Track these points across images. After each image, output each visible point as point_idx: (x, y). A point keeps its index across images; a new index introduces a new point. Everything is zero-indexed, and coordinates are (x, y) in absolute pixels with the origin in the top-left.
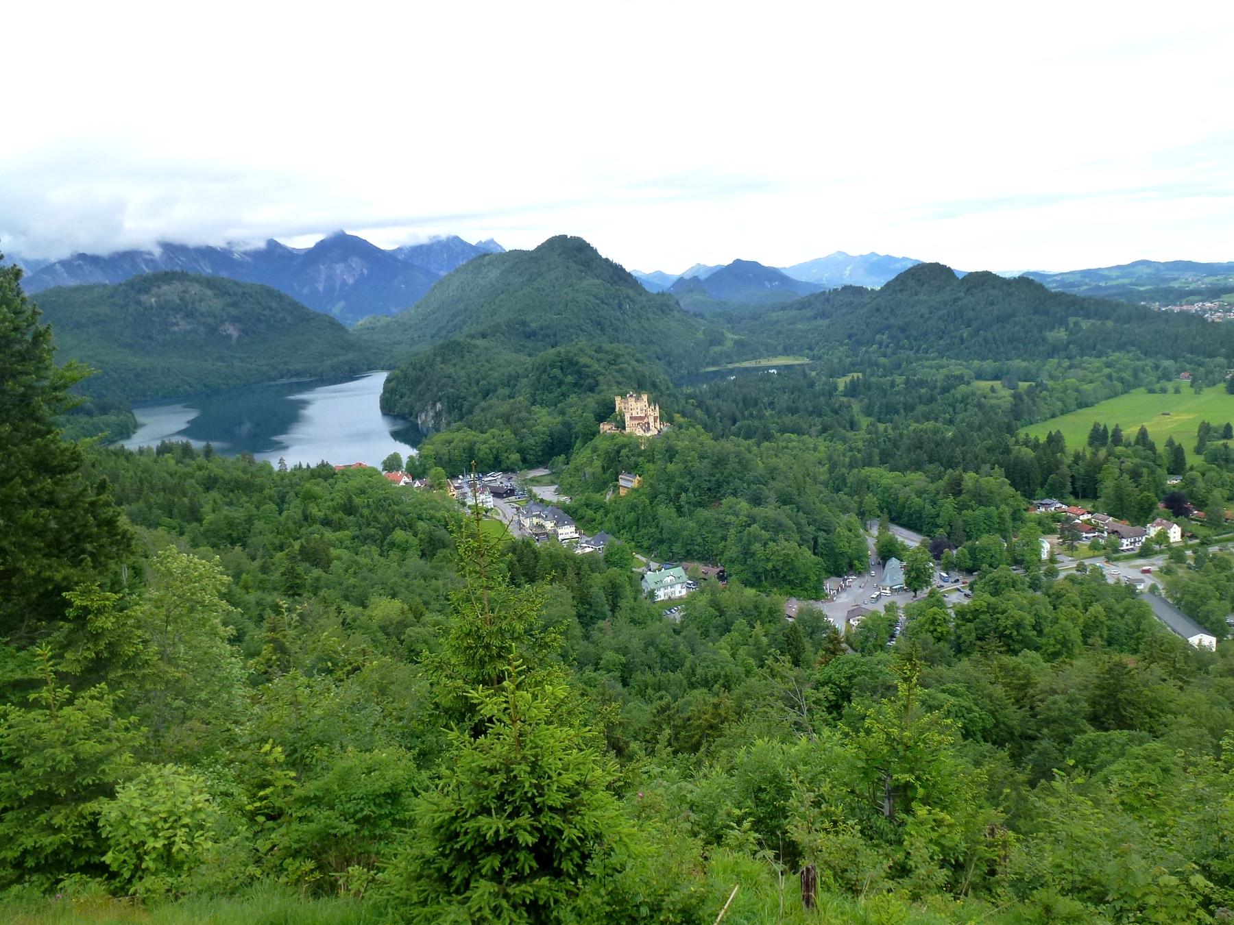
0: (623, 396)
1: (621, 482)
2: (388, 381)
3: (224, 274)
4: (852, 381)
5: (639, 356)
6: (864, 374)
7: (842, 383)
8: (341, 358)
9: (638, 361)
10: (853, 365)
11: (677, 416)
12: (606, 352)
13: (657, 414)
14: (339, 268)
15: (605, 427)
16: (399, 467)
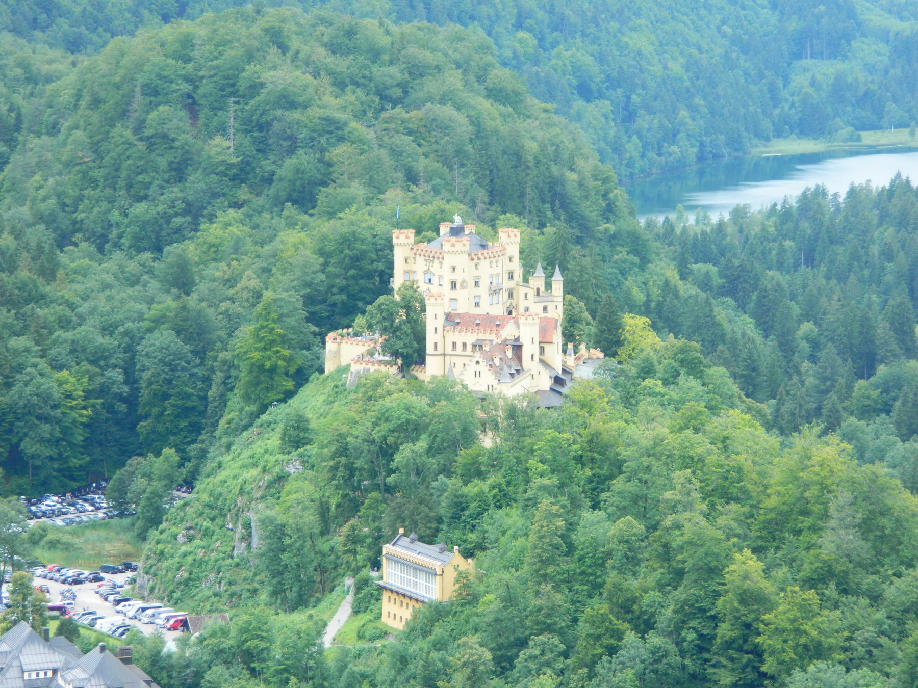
0: (426, 229)
1: (391, 575)
5: (501, 75)
9: (496, 94)
11: (634, 324)
12: (375, 54)
13: (557, 312)
15: (349, 353)
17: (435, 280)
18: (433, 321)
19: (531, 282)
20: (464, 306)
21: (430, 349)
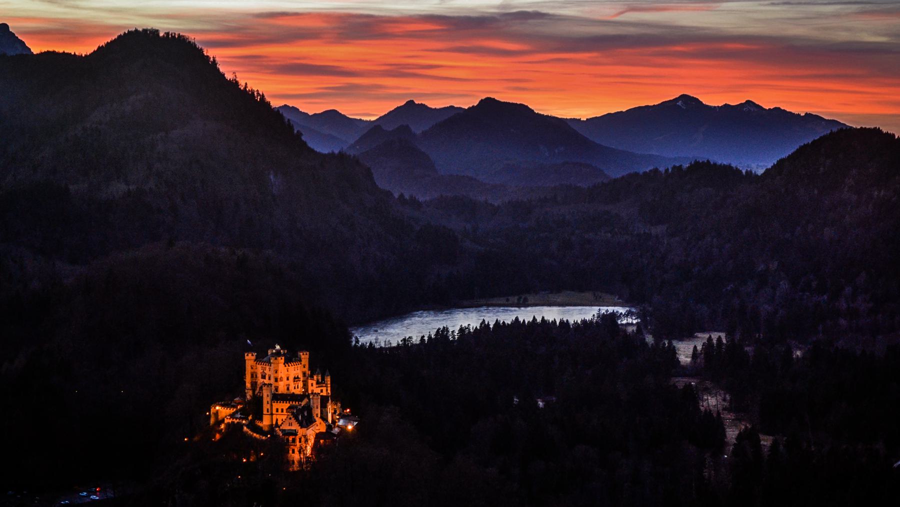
13: (326, 391)
17: (267, 377)
19: (315, 377)
20: (282, 389)
21: (265, 412)
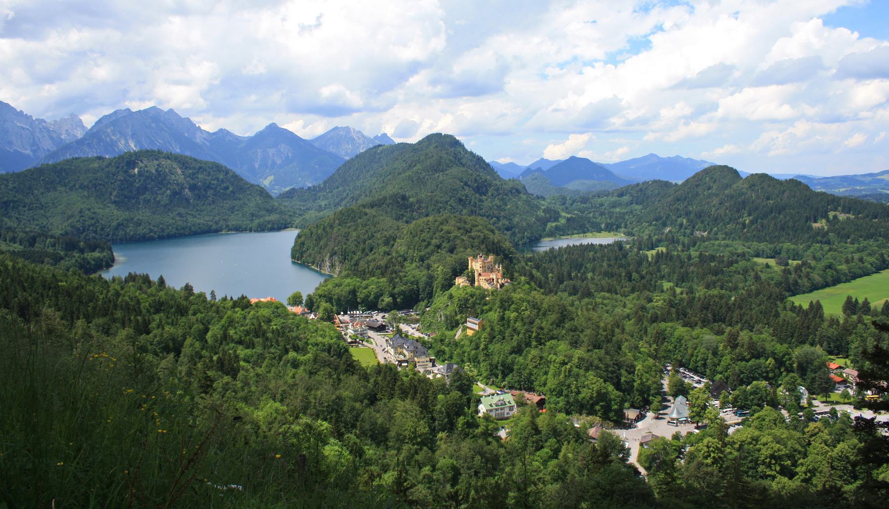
2: (299, 236)
3: (188, 153)
4: (658, 254)
6: (667, 249)
7: (651, 254)
8: (267, 218)
10: (659, 241)
11: (516, 274)
14: (271, 151)
15: (460, 281)
16: (301, 303)
18: (476, 275)
